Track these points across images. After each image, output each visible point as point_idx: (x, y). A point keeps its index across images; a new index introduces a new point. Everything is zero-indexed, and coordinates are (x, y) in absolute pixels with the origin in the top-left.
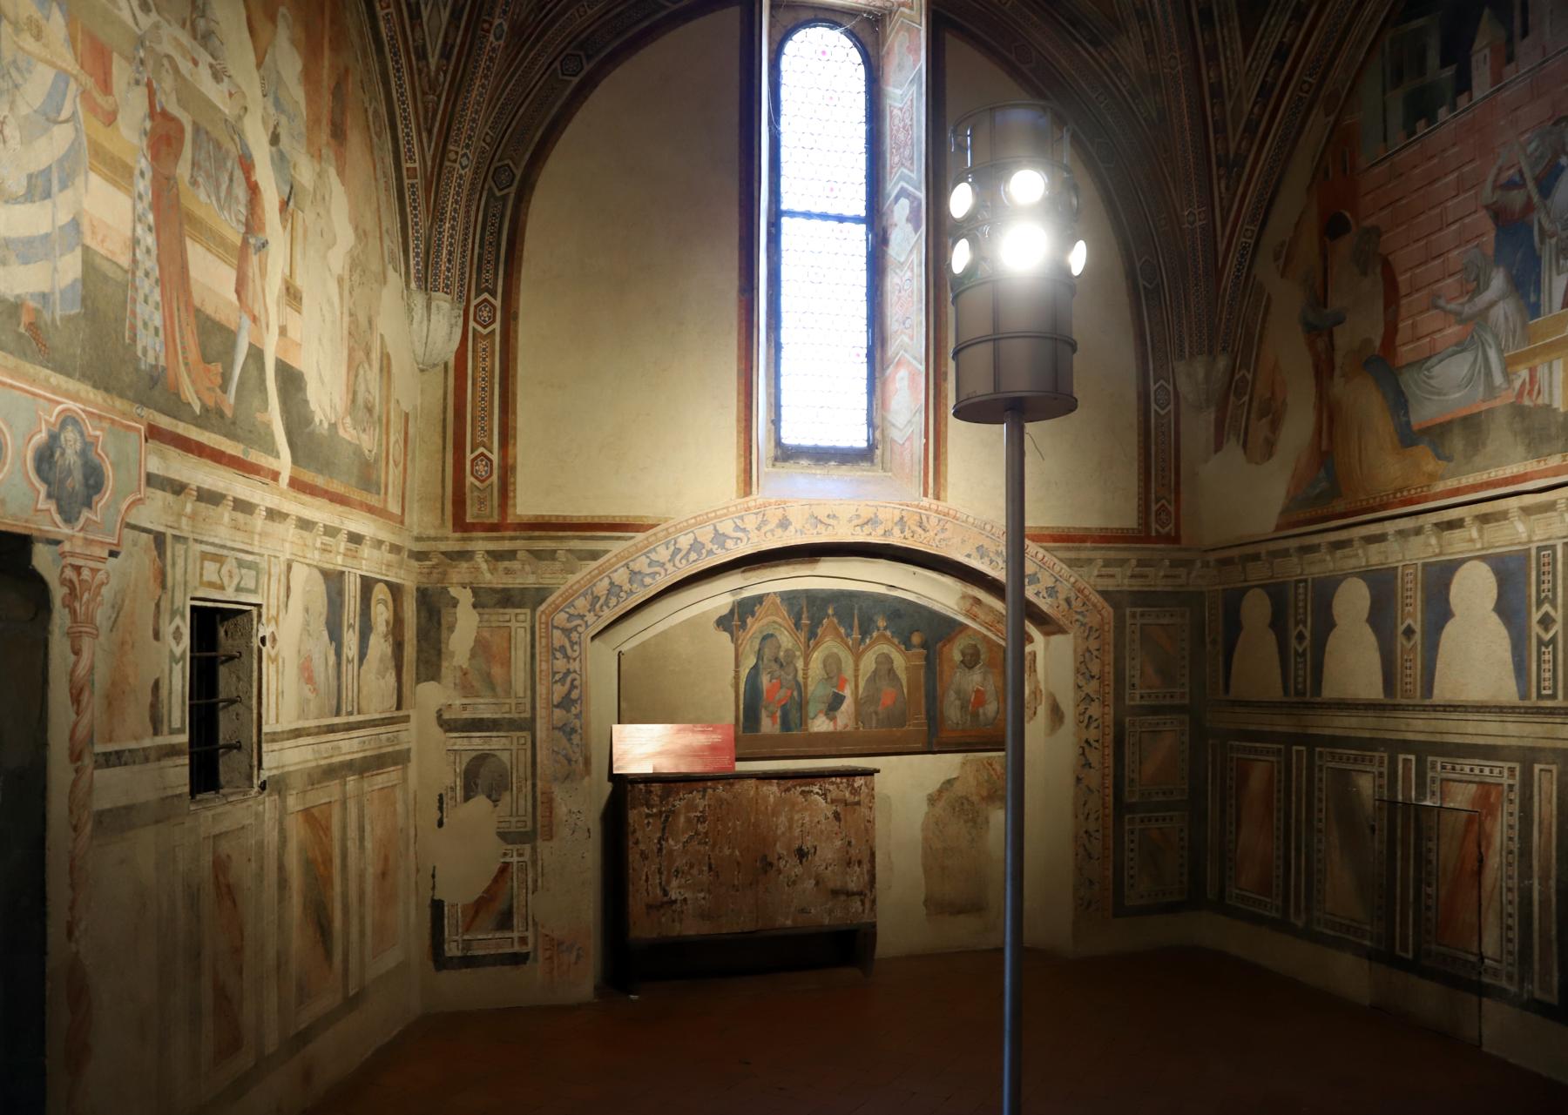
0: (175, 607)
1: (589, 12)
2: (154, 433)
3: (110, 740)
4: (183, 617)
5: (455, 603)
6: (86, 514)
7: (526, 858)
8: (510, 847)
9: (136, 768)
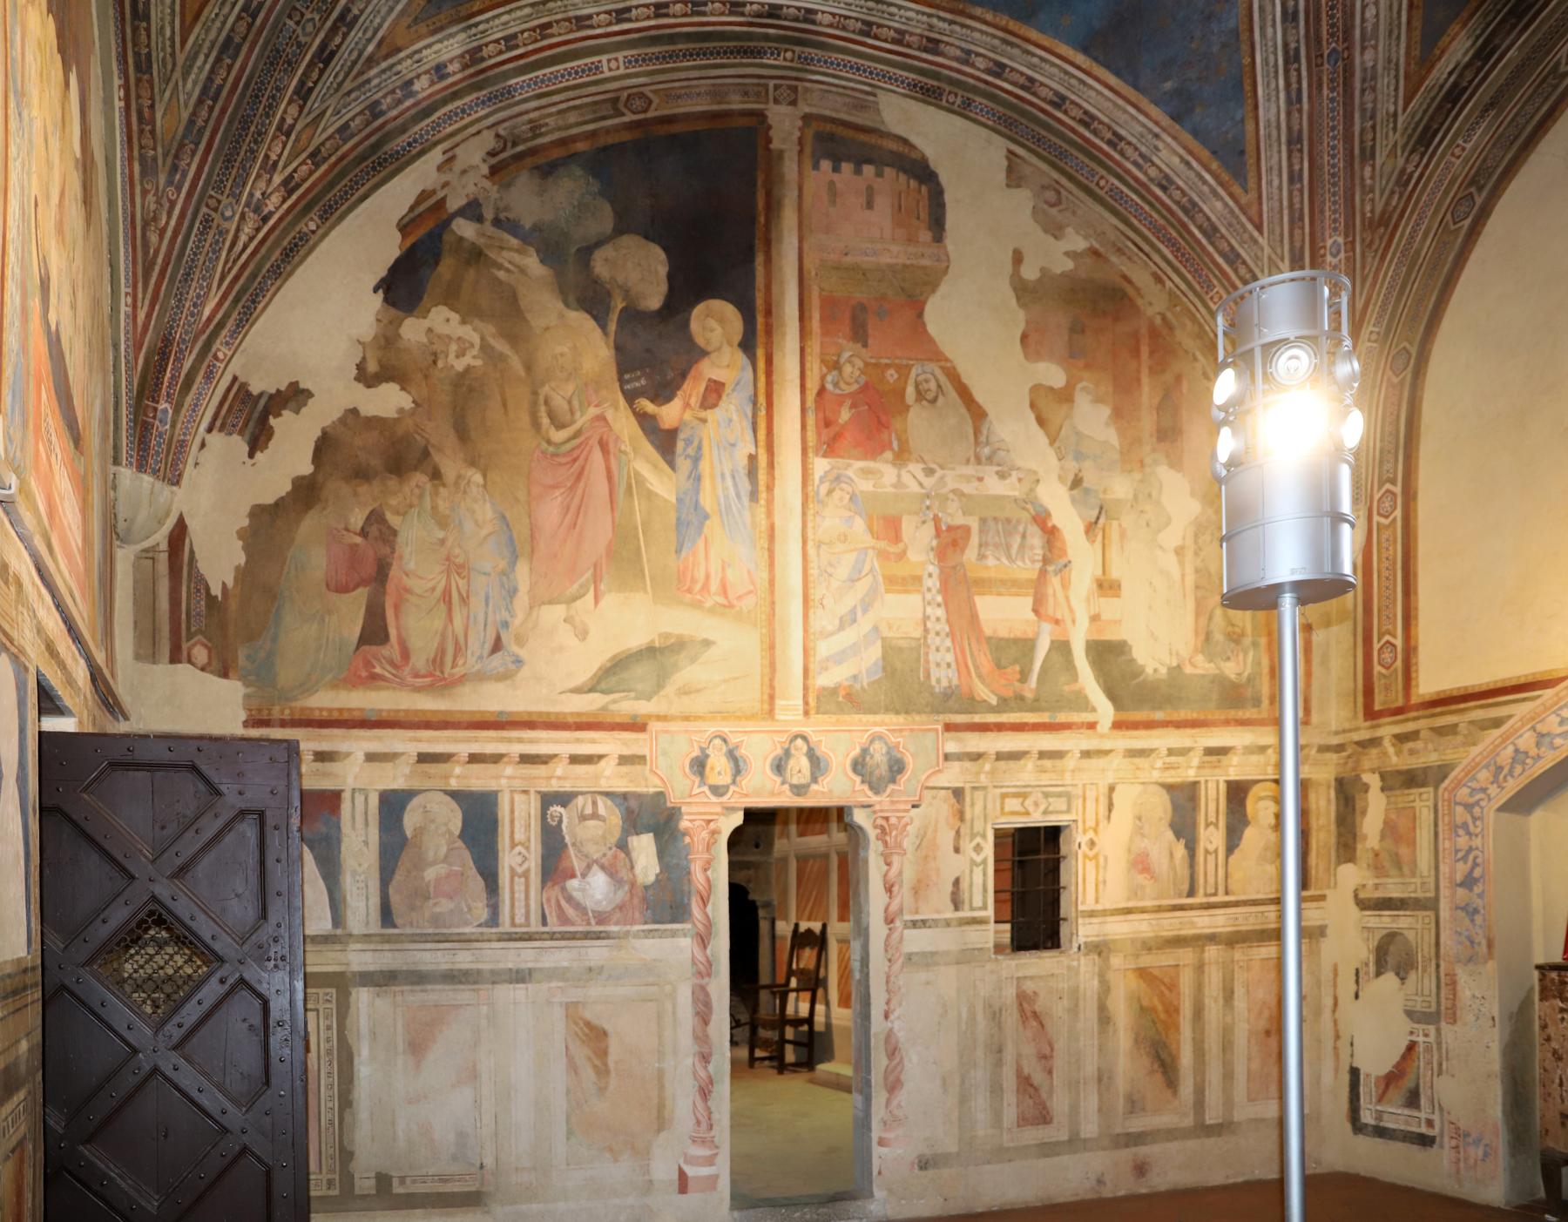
1: (1469, 146)
2: (949, 727)
3: (917, 912)
4: (984, 836)
5: (1366, 788)
6: (891, 787)
7: (1432, 1039)
8: (1416, 1026)
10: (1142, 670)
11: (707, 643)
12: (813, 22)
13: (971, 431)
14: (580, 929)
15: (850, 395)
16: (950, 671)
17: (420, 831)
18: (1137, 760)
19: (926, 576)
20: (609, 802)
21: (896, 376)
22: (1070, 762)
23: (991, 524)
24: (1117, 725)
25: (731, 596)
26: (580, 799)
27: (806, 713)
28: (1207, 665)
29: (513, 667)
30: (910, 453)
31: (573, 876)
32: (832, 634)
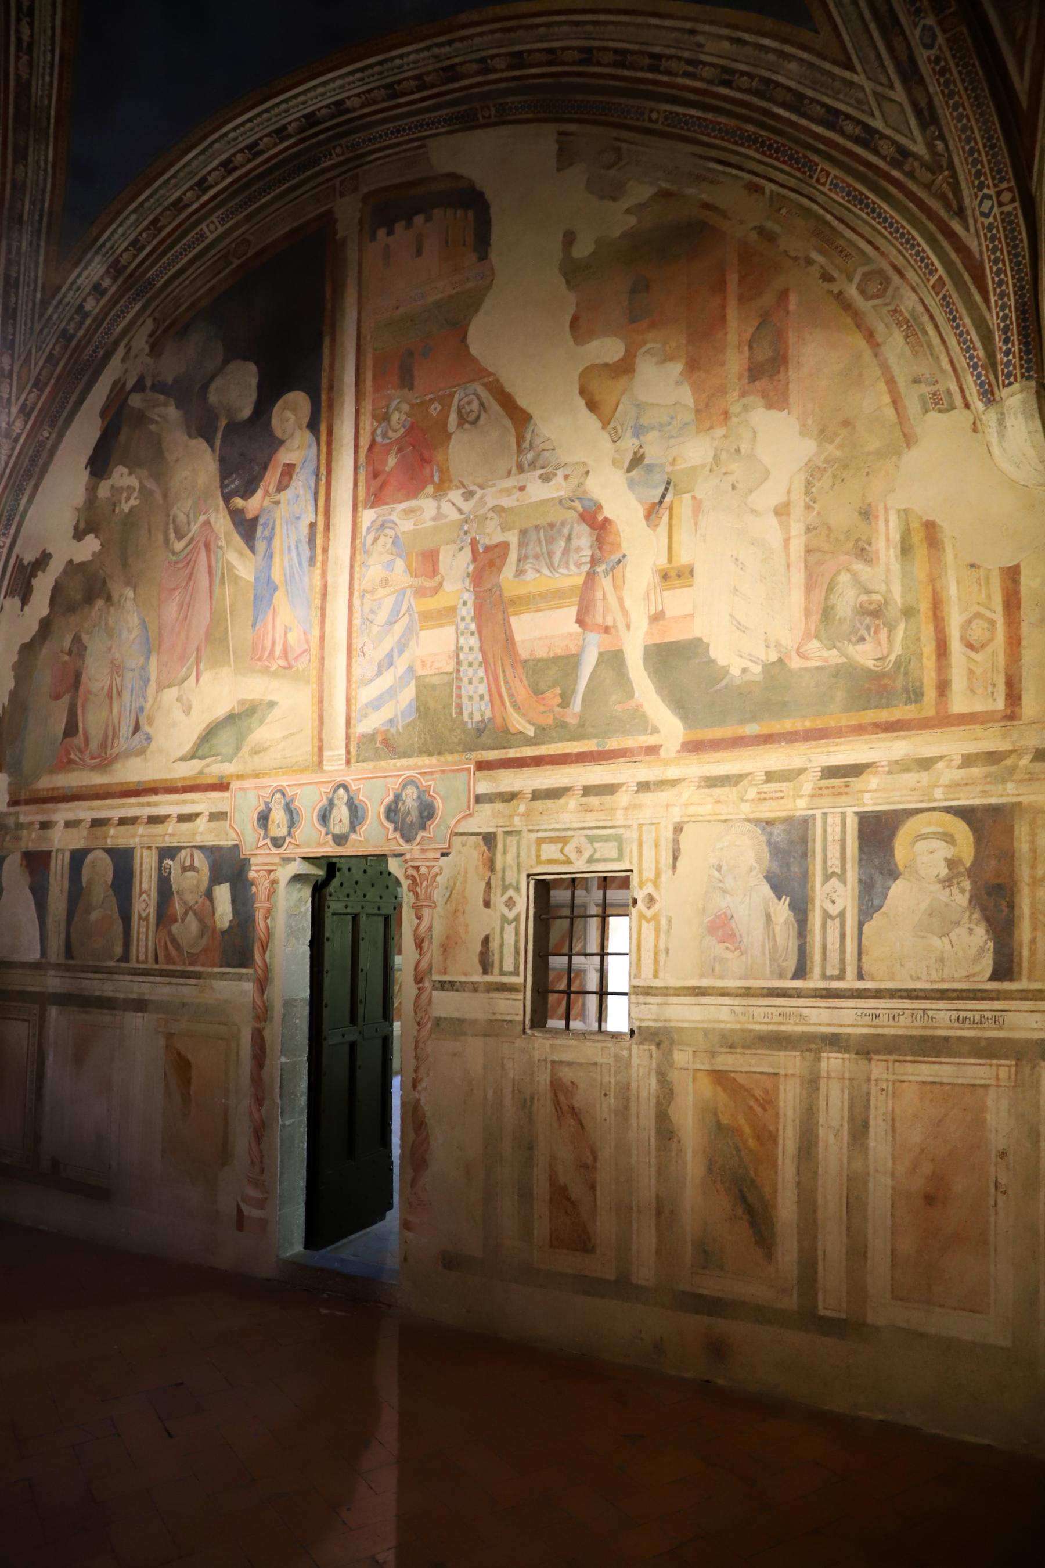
0: (507, 883)
3: (445, 973)
4: (517, 889)
6: (421, 834)
9: (466, 995)
10: (725, 671)
11: (272, 704)
12: (348, 111)
13: (513, 440)
14: (179, 968)
15: (397, 441)
16: (482, 703)
17: (90, 881)
18: (717, 791)
19: (460, 606)
20: (202, 855)
21: (439, 408)
22: (623, 798)
23: (533, 535)
25: (291, 656)
26: (183, 852)
27: (348, 762)
28: (825, 653)
29: (145, 743)
30: (450, 481)
31: (176, 921)
32: (372, 680)
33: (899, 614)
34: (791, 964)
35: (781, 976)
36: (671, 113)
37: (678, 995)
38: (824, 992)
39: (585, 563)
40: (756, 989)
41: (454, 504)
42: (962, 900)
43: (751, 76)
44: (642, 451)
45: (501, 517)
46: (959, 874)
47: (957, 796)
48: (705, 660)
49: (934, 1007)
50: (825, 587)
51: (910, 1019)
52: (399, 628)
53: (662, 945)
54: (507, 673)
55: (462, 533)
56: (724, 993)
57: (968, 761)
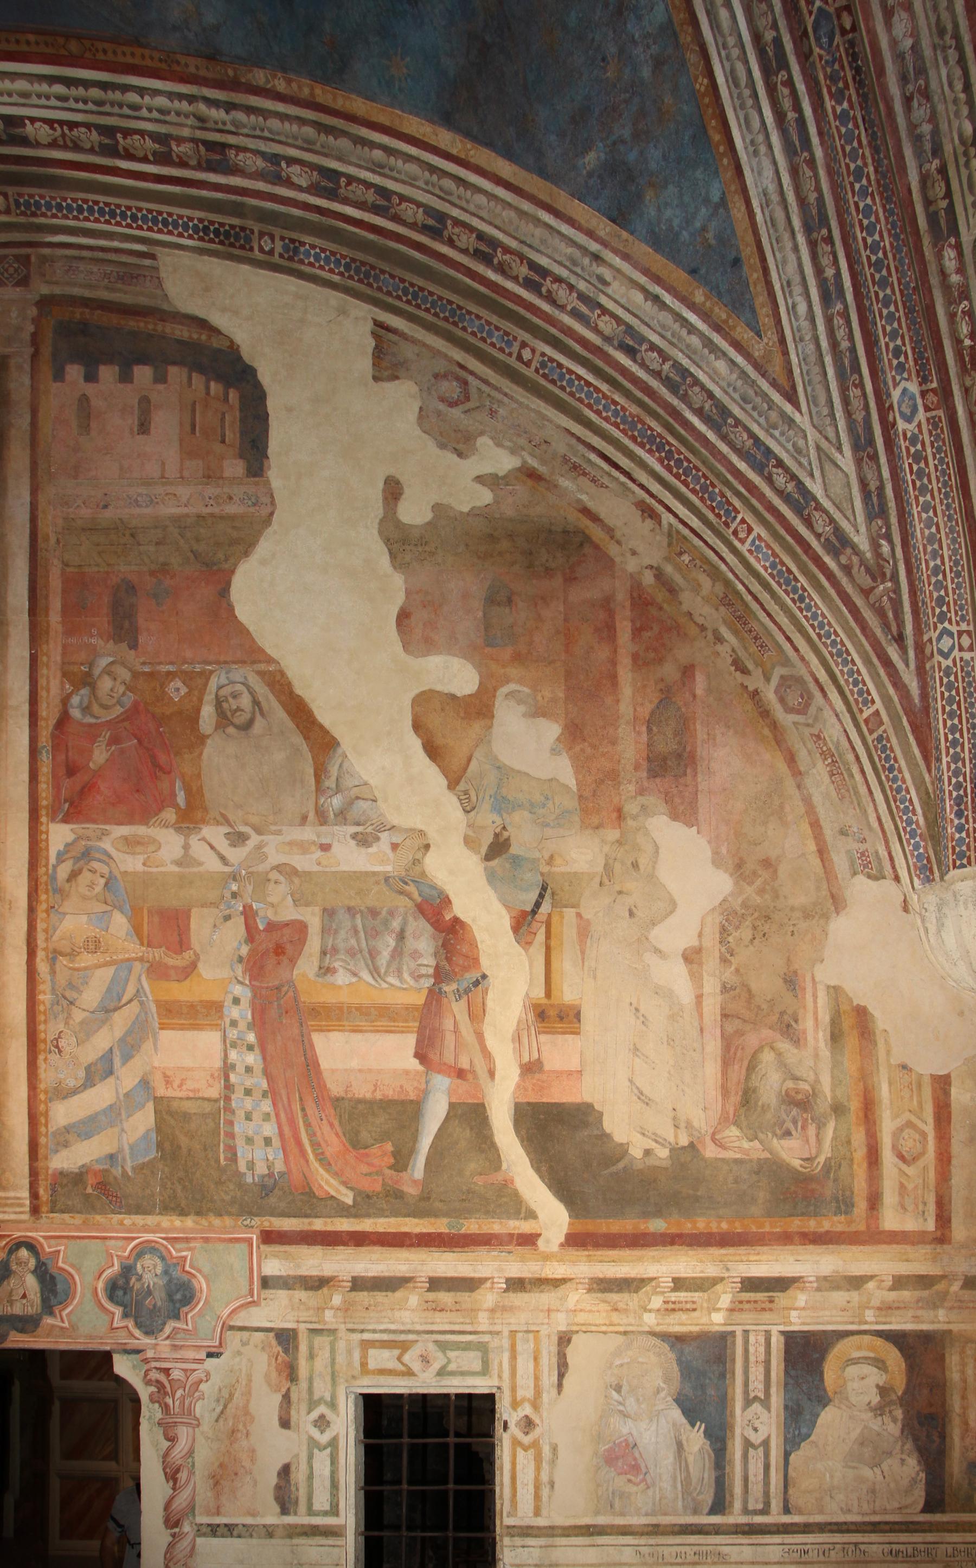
0: (316, 1397)
2: (269, 1237)
3: (218, 1514)
4: (333, 1405)
9: (254, 1541)
10: (623, 1150)
13: (311, 771)
16: (269, 1149)
18: (614, 1297)
19: (228, 1002)
21: (184, 690)
22: (487, 1298)
24: (575, 1240)
27: (35, 1210)
28: (746, 1145)
30: (206, 810)
32: (75, 1092)
33: (829, 1110)
34: (708, 1498)
35: (696, 1512)
36: (551, 360)
37: (568, 1536)
38: (747, 1528)
39: (427, 976)
40: (666, 1526)
41: (212, 847)
42: (894, 1429)
43: (664, 357)
44: (506, 834)
45: (292, 882)
46: (891, 1403)
47: (888, 1320)
48: (596, 1132)
49: (866, 1539)
50: (746, 1063)
51: (841, 1554)
52: (121, 1021)
53: (544, 1477)
54: (309, 1112)
55: (228, 895)
56: (625, 1531)
57: (899, 1282)
